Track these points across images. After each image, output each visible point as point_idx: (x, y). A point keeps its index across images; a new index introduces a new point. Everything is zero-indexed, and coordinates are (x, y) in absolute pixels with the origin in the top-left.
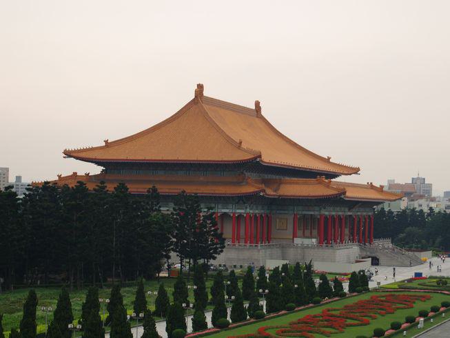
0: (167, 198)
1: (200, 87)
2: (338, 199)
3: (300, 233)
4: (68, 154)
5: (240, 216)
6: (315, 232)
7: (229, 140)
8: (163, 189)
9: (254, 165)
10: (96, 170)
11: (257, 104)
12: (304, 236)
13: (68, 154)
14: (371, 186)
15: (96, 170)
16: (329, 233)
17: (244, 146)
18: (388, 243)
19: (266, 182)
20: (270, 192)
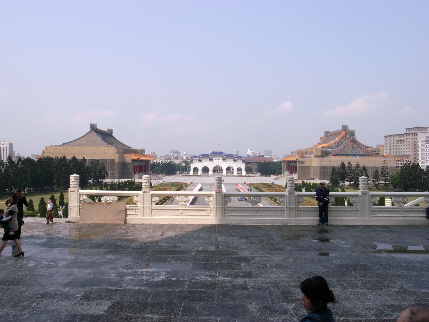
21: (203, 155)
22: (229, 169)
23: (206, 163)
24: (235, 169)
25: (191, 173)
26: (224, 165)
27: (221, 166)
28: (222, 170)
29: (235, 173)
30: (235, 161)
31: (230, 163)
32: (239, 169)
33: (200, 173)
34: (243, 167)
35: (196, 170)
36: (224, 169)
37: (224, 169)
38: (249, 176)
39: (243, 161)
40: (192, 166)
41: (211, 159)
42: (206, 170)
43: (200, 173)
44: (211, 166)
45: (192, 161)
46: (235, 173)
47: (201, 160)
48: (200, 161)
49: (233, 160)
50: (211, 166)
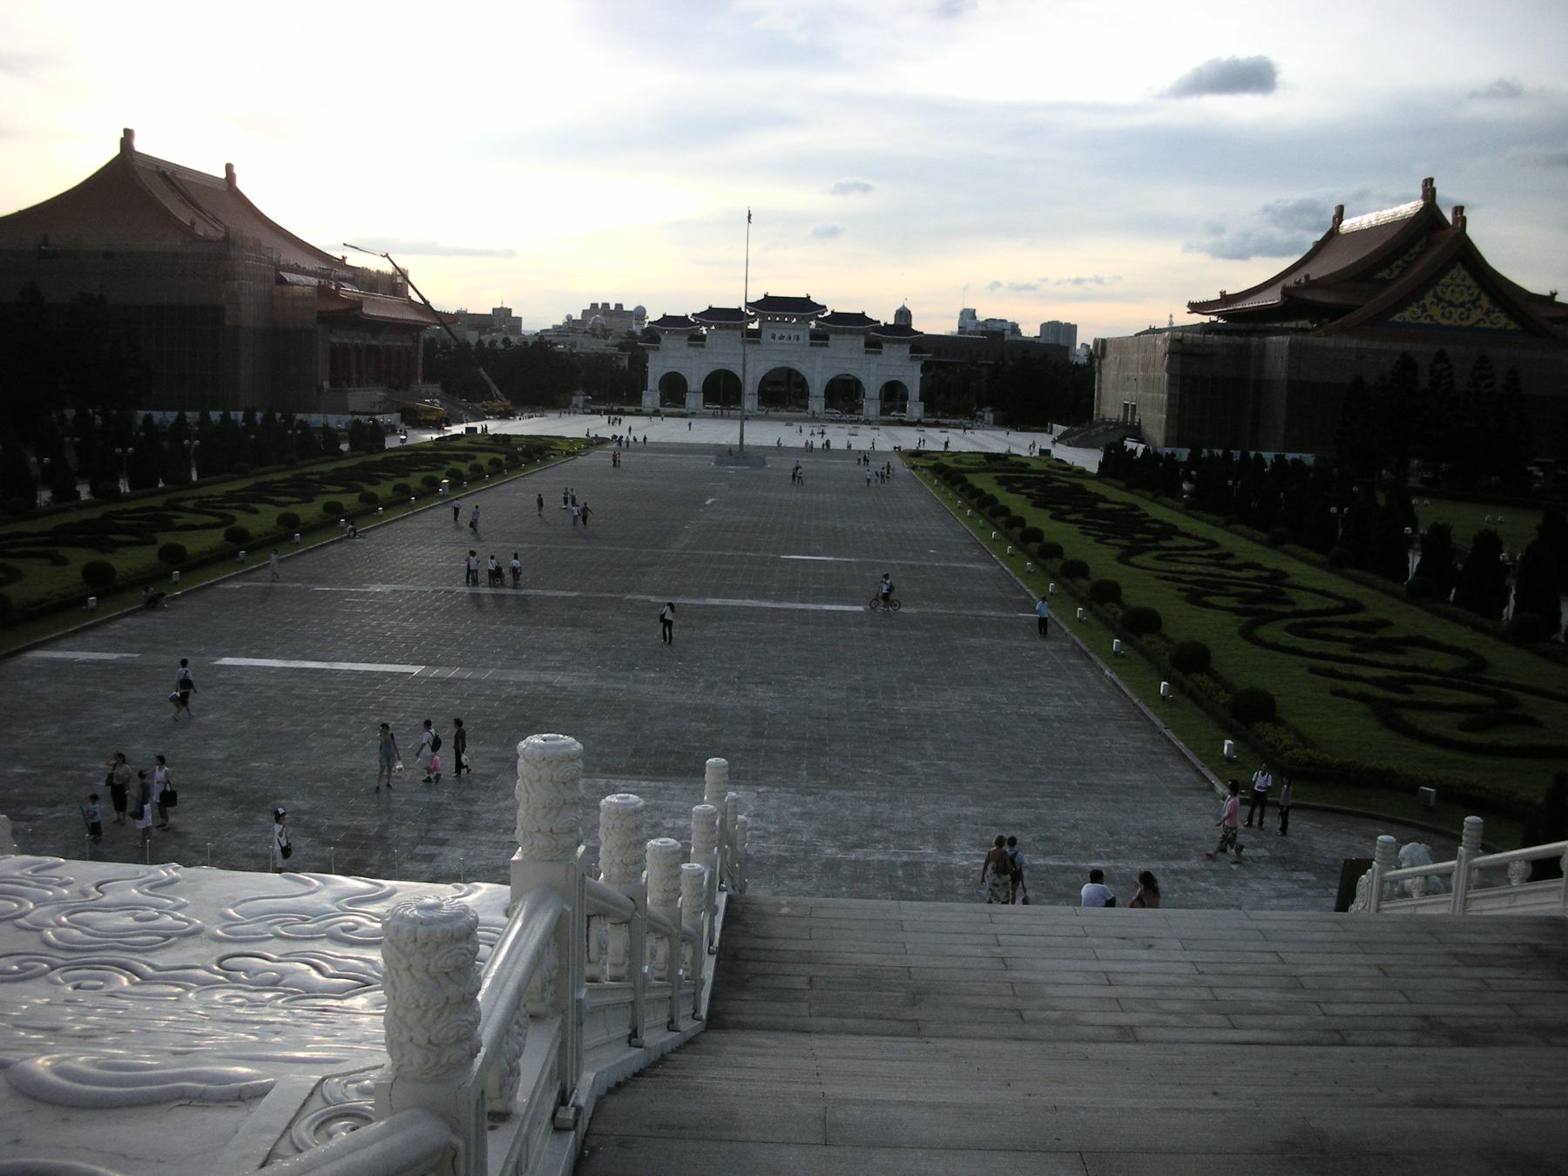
21: (712, 314)
24: (872, 387)
25: (651, 398)
26: (818, 371)
27: (803, 368)
29: (871, 408)
30: (873, 345)
32: (893, 395)
33: (694, 401)
34: (912, 378)
35: (674, 390)
36: (817, 386)
37: (817, 386)
40: (657, 368)
43: (694, 401)
44: (753, 369)
45: (656, 339)
46: (871, 408)
48: (697, 339)
49: (862, 341)
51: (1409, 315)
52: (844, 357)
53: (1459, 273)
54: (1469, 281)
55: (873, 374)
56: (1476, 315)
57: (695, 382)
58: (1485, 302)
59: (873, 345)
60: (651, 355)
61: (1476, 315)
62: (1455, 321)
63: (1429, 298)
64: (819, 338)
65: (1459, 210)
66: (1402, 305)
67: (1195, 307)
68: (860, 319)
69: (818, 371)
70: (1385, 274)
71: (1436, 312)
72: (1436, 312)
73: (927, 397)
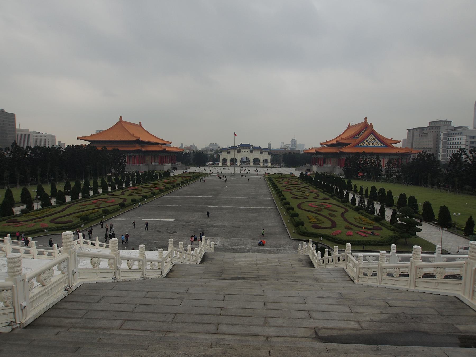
0: (109, 151)
1: (121, 117)
2: (164, 151)
3: (153, 161)
4: (78, 138)
5: (135, 156)
6: (158, 161)
7: (131, 134)
8: (108, 149)
9: (138, 142)
10: (88, 143)
11: (140, 123)
12: (155, 162)
13: (78, 138)
14: (175, 147)
15: (89, 143)
16: (162, 161)
17: (135, 136)
18: (180, 163)
19: (142, 146)
20: (143, 149)
22: (256, 161)
23: (233, 154)
24: (261, 160)
25: (220, 164)
28: (249, 161)
30: (261, 152)
31: (256, 154)
32: (266, 161)
33: (228, 164)
34: (269, 158)
35: (225, 161)
36: (251, 160)
37: (251, 160)
38: (273, 167)
39: (269, 153)
40: (221, 158)
41: (239, 151)
42: (233, 161)
43: (228, 164)
45: (221, 152)
46: (261, 164)
47: (230, 152)
48: (229, 152)
50: (239, 157)
51: (362, 144)
52: (256, 154)
53: (372, 136)
54: (374, 137)
55: (262, 157)
56: (375, 144)
57: (229, 160)
58: (377, 141)
59: (261, 152)
60: (221, 156)
61: (375, 144)
62: (371, 145)
63: (366, 141)
64: (251, 151)
65: (371, 124)
66: (360, 142)
67: (321, 144)
68: (258, 148)
69: (251, 157)
70: (357, 136)
71: (367, 143)
72: (367, 143)
73: (272, 162)
